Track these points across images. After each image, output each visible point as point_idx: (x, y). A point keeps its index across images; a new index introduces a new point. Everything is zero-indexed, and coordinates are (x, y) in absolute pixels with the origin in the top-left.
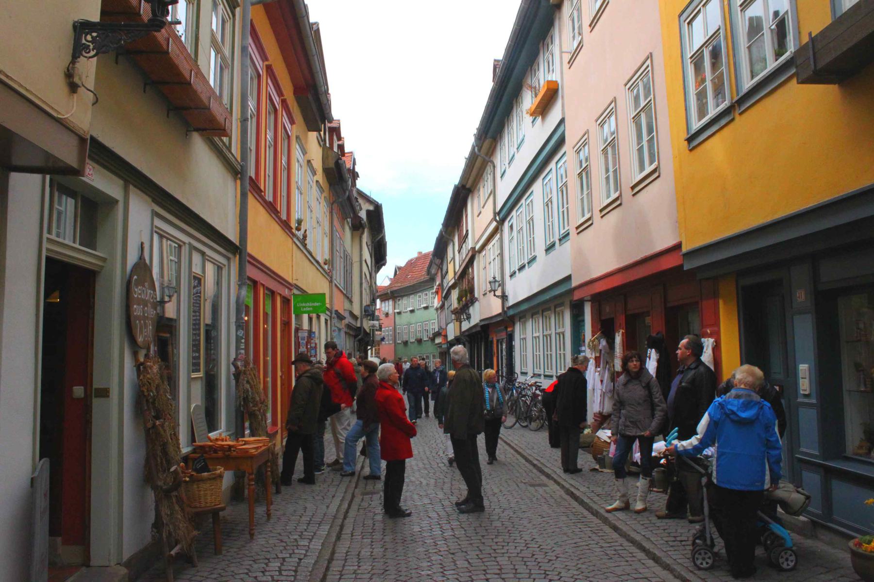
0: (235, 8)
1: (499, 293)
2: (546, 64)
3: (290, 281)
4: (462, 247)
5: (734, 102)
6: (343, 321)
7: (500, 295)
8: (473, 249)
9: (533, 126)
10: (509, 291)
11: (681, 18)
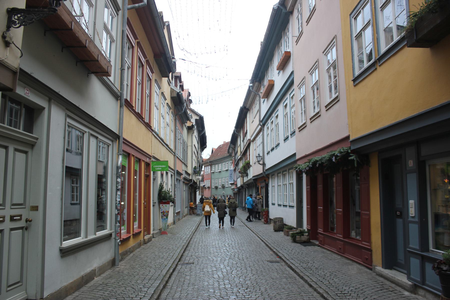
0: (118, 11)
1: (261, 162)
2: (285, 43)
3: (150, 154)
4: (244, 139)
5: (376, 59)
6: (182, 176)
7: (262, 163)
8: (249, 140)
9: (279, 75)
10: (266, 162)
11: (351, 16)
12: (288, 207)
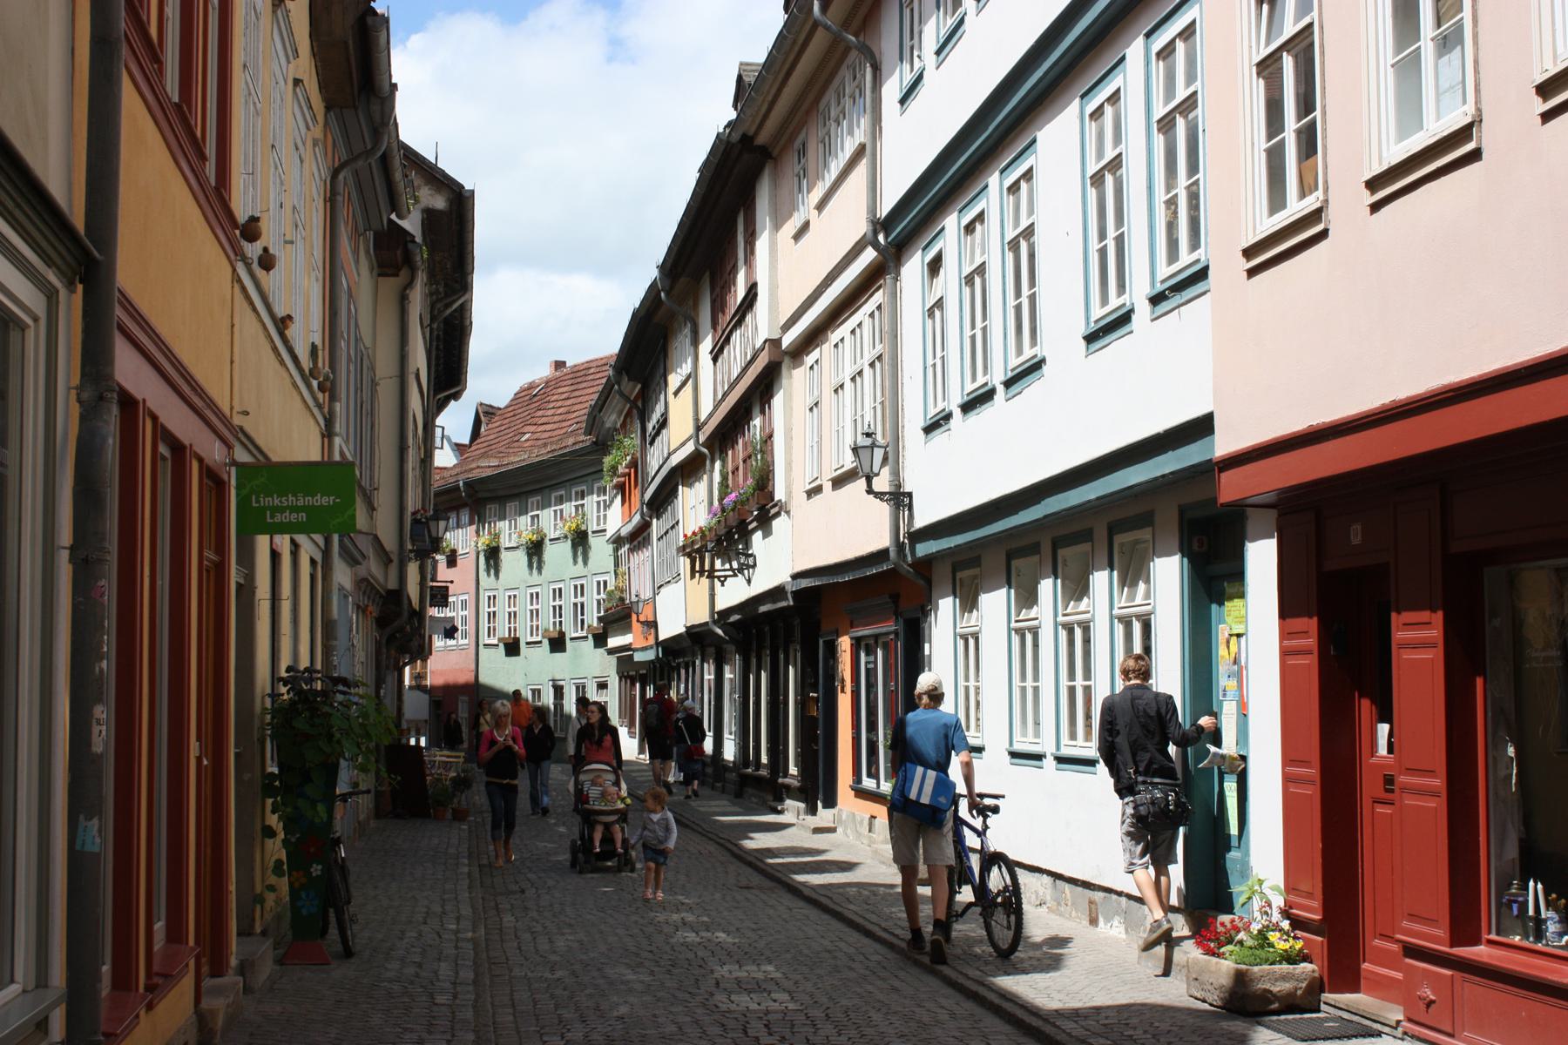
4: (727, 340)
7: (886, 489)
8: (775, 343)
12: (1049, 762)
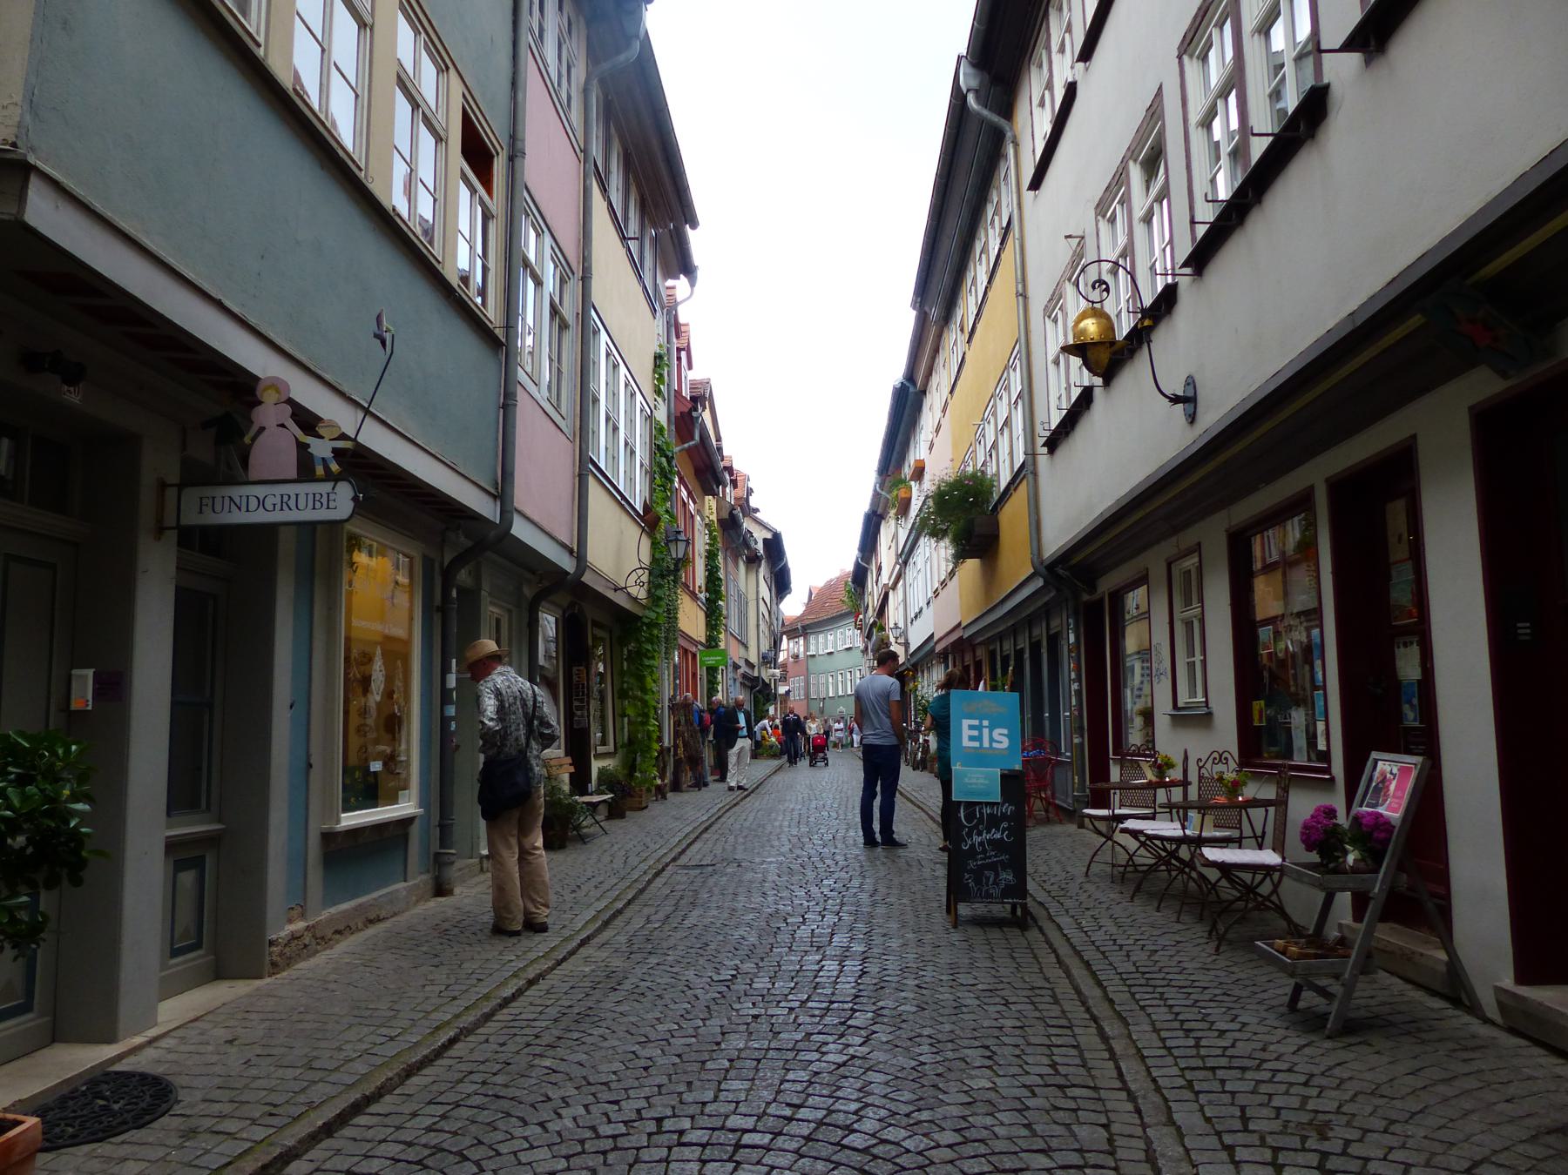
10: (911, 640)
